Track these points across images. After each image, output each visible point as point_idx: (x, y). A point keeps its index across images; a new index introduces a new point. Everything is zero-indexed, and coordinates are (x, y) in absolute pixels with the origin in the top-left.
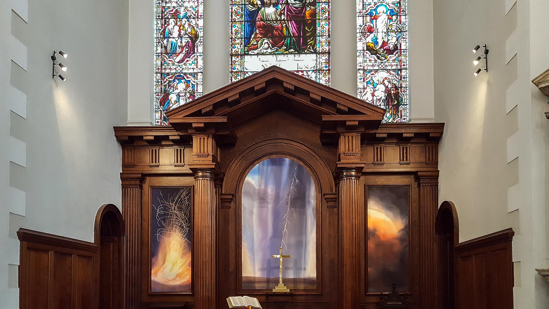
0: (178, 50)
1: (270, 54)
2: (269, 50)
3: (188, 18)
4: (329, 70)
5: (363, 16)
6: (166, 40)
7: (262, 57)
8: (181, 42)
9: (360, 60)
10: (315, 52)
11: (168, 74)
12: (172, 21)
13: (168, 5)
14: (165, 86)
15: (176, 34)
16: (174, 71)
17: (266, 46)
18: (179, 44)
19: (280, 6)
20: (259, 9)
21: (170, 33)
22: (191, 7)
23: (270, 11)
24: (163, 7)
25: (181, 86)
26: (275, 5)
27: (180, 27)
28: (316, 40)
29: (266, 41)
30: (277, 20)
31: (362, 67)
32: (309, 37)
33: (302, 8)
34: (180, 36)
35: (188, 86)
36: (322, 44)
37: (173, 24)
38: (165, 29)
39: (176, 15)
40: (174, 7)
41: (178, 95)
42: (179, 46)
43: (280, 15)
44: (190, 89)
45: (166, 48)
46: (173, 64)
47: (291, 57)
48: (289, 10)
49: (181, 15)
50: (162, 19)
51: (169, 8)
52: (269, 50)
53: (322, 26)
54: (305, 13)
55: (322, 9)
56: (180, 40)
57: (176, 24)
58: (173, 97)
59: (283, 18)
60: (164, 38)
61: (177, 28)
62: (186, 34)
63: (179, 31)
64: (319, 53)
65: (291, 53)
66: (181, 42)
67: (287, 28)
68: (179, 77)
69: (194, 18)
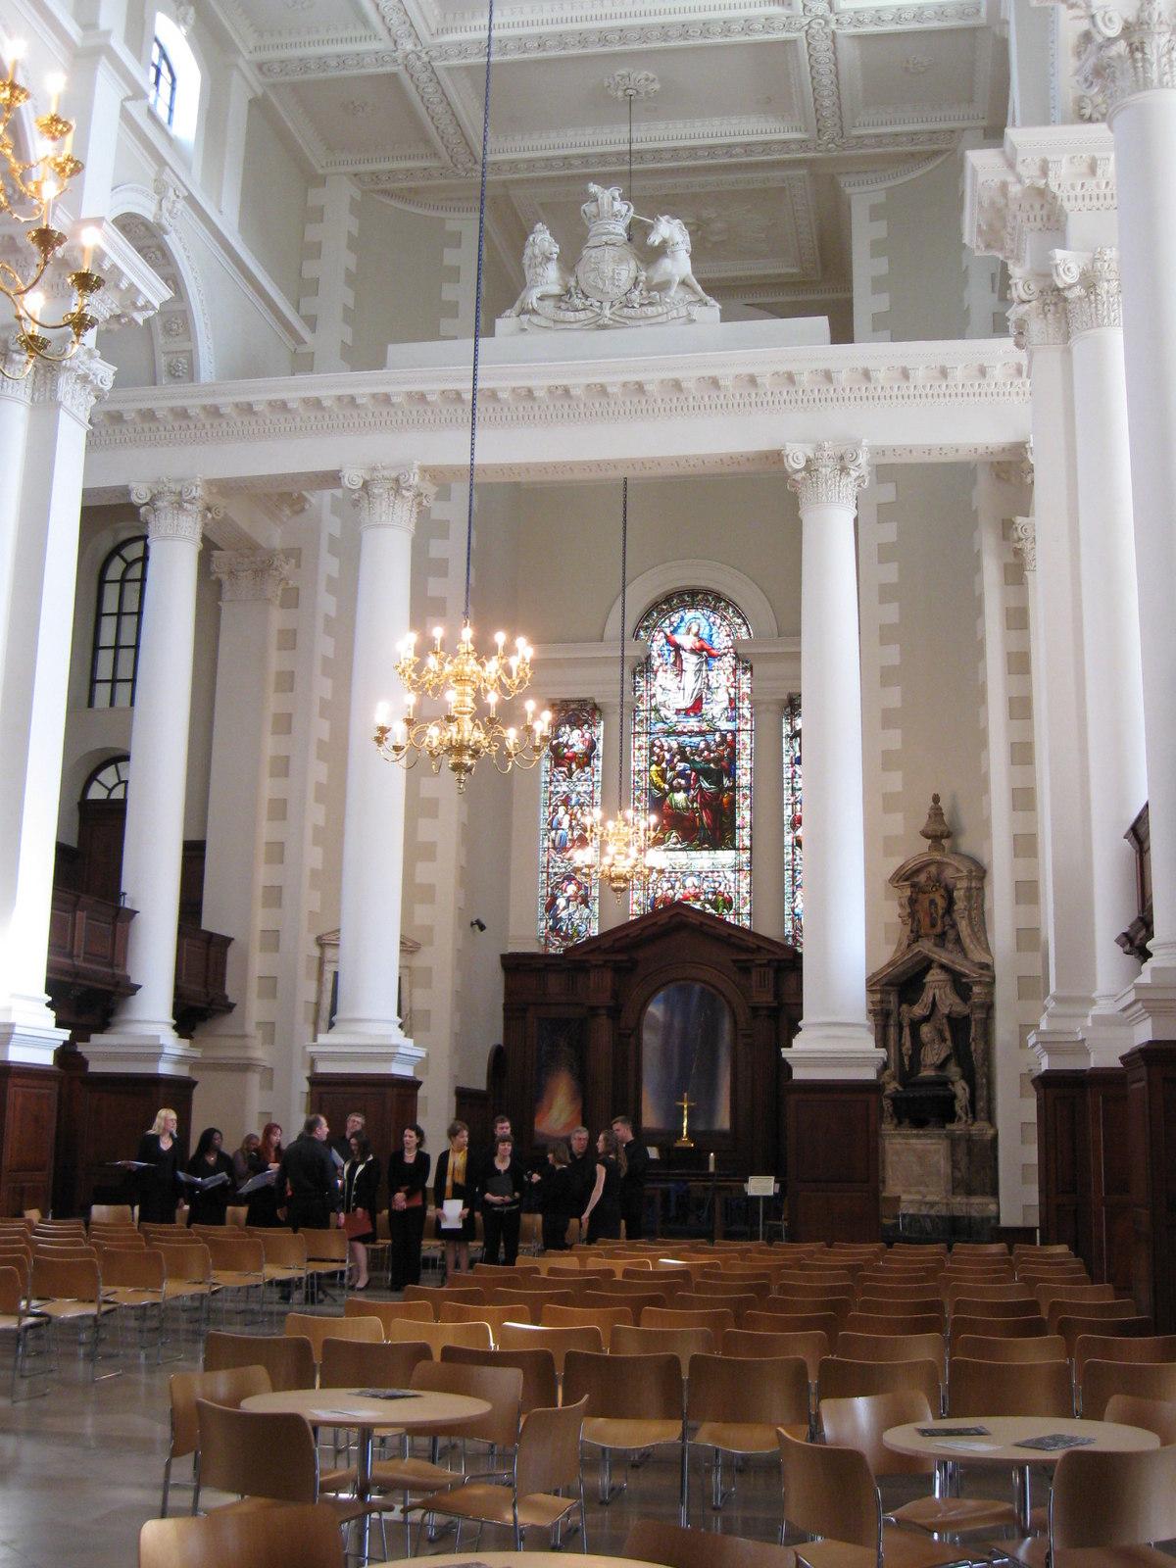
0: (569, 844)
1: (680, 850)
2: (679, 846)
3: (581, 805)
4: (750, 870)
5: (792, 804)
6: (554, 832)
7: (671, 854)
8: (572, 835)
9: (788, 858)
10: (735, 848)
11: (556, 874)
12: (562, 810)
13: (557, 789)
14: (552, 888)
15: (565, 824)
16: (564, 870)
17: (675, 840)
18: (570, 837)
19: (692, 792)
20: (667, 795)
21: (560, 824)
22: (585, 792)
23: (680, 798)
24: (551, 792)
25: (571, 889)
26: (687, 790)
27: (571, 815)
28: (735, 833)
29: (674, 834)
30: (687, 808)
31: (791, 867)
32: (727, 830)
33: (718, 794)
34: (571, 827)
35: (579, 889)
36: (743, 837)
37: (564, 813)
38: (553, 819)
39: (566, 802)
40: (564, 792)
41: (568, 900)
42: (570, 840)
43: (692, 803)
44: (582, 892)
45: (554, 841)
46: (562, 862)
47: (705, 853)
48: (703, 797)
49: (573, 802)
50: (550, 805)
51: (558, 793)
52: (679, 846)
53: (743, 816)
54: (722, 800)
55: (743, 795)
56: (570, 833)
57: (566, 813)
58: (561, 902)
59: (695, 805)
60: (553, 829)
61: (567, 817)
62: (578, 825)
63: (571, 821)
64: (738, 849)
65: (705, 849)
66: (572, 835)
67: (701, 819)
68: (569, 878)
69: (588, 806)
